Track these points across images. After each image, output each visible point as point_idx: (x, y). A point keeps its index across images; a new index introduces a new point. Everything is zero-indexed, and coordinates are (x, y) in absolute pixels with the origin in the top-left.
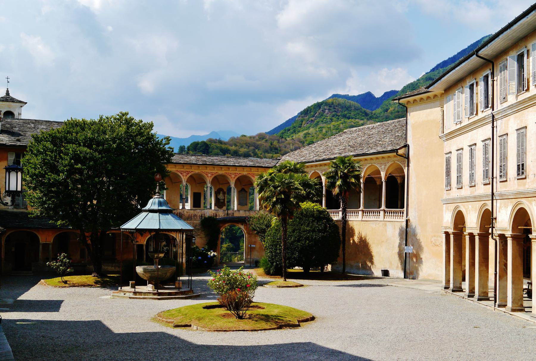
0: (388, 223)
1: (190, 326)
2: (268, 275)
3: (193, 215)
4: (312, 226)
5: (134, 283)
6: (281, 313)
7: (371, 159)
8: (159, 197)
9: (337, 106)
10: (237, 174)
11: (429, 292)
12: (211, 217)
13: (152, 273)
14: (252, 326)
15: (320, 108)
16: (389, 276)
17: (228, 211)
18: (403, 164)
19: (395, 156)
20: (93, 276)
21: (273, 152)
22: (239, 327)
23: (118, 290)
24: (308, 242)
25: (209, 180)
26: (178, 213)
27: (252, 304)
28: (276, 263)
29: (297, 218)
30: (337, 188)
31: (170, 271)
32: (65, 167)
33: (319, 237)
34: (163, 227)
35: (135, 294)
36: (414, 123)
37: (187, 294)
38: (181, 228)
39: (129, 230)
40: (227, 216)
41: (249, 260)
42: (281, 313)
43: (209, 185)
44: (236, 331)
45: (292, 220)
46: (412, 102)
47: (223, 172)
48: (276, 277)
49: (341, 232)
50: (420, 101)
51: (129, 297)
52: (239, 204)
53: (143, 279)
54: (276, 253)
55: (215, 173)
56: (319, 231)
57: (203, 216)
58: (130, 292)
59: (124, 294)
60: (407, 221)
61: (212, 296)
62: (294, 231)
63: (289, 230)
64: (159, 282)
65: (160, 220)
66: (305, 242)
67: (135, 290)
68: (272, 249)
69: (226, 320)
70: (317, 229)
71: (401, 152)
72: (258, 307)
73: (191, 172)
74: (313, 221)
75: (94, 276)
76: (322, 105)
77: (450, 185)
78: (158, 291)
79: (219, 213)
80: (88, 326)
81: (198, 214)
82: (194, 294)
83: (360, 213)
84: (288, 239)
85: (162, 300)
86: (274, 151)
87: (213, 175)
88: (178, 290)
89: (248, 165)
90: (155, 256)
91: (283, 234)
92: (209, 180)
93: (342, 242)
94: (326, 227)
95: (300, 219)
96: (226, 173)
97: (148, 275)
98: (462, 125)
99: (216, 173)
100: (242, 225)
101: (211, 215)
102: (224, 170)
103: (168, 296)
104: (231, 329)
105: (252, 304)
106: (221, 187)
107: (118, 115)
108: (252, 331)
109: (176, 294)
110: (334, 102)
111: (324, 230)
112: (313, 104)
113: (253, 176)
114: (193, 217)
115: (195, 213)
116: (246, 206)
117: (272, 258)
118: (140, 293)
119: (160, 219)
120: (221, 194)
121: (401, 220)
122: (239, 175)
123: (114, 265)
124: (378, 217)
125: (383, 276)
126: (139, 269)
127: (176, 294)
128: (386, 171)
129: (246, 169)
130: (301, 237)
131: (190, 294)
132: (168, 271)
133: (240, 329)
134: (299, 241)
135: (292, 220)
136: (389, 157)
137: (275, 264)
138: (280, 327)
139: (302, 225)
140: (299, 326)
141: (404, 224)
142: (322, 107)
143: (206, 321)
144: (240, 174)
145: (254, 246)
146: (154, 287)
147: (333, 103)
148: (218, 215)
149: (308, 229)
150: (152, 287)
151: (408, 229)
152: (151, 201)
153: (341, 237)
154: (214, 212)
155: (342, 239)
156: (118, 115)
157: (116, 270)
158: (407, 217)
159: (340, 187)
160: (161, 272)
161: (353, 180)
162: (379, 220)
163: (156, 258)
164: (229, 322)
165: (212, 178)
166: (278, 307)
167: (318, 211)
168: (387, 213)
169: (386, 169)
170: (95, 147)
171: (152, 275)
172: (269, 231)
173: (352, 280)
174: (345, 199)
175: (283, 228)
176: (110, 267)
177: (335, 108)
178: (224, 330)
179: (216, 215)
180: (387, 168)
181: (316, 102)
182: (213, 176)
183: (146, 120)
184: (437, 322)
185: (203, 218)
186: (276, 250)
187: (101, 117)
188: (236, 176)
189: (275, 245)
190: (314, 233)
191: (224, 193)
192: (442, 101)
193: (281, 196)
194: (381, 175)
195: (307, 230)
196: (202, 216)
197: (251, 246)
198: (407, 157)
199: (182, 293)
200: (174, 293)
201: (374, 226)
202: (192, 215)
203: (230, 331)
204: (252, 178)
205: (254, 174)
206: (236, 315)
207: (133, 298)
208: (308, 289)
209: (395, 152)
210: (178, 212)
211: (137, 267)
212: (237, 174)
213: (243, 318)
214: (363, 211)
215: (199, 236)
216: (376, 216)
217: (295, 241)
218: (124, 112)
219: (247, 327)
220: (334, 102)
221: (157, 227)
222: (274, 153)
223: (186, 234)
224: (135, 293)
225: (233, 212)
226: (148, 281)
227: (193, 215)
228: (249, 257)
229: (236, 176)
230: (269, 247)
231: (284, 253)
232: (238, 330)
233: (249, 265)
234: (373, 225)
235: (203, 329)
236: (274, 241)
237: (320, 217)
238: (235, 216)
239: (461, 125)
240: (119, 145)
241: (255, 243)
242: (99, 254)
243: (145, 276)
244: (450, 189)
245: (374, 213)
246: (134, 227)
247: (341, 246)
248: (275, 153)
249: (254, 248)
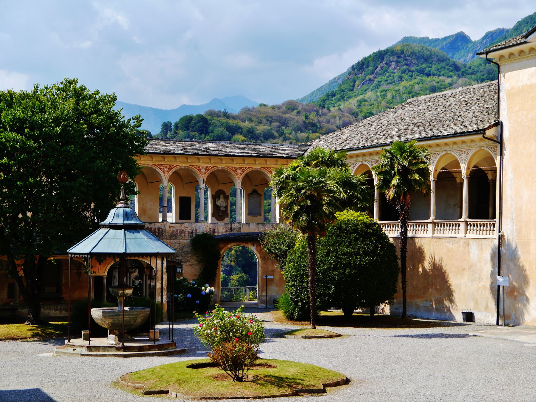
0: (471, 242)
1: (167, 392)
2: (291, 320)
3: (178, 232)
4: (355, 247)
5: (89, 333)
6: (299, 374)
7: (446, 144)
8: (124, 205)
9: (409, 56)
10: (244, 168)
11: (530, 346)
12: (206, 233)
13: (114, 317)
14: (254, 392)
15: (382, 59)
16: (474, 322)
17: (231, 225)
18: (494, 151)
19: (481, 139)
20: (27, 325)
21: (309, 130)
22: (237, 393)
24: (348, 270)
25: (202, 179)
26: (157, 229)
27: (258, 362)
28: (302, 301)
29: (333, 234)
30: (392, 189)
31: (141, 315)
33: (365, 262)
34: (130, 251)
35: (89, 350)
36: (509, 89)
37: (166, 349)
38: (157, 252)
39: (81, 256)
40: (231, 232)
41: (264, 298)
42: (299, 374)
43: (203, 185)
44: (232, 398)
45: (325, 238)
46: (507, 57)
47: (224, 166)
48: (303, 323)
49: (399, 254)
50: (519, 56)
51: (81, 354)
52: (250, 213)
53: (101, 327)
54: (302, 287)
55: (212, 168)
56: (366, 253)
57: (193, 232)
58: (83, 346)
59: (74, 350)
60: (501, 238)
61: (203, 352)
62: (327, 254)
63: (321, 251)
64: (125, 331)
65: (127, 240)
66: (345, 270)
67: (89, 344)
68: (296, 281)
69: (218, 383)
70: (363, 252)
71: (489, 133)
72: (267, 365)
73: (175, 167)
74: (357, 239)
75: (29, 324)
76: (386, 56)
78: (123, 345)
79: (218, 227)
80: (19, 394)
81: (187, 230)
82: (177, 347)
83: (430, 226)
84: (320, 267)
85: (129, 357)
86: (311, 130)
87: (208, 170)
88: (153, 343)
89: (262, 155)
90: (119, 293)
91: (310, 258)
92: (202, 179)
93: (400, 270)
94: (376, 247)
95: (338, 235)
96: (229, 167)
97: (109, 321)
99: (214, 167)
100: (253, 245)
101: (207, 231)
102: (225, 163)
103: (138, 351)
104: (224, 397)
105: (258, 362)
106: (221, 187)
107: (62, 83)
108: (255, 398)
109: (150, 348)
110: (406, 49)
111: (373, 253)
112: (371, 53)
113: (269, 172)
114: (178, 235)
115: (182, 228)
116: (259, 217)
117: (295, 295)
118: (98, 348)
119: (126, 238)
120: (222, 199)
121: (491, 236)
122: (249, 170)
123: (59, 307)
124: (457, 231)
125: (464, 321)
126: (96, 313)
127: (150, 348)
128: (467, 162)
129: (258, 161)
130: (339, 262)
131: (170, 348)
132: (138, 314)
133: (238, 396)
134: (335, 269)
135: (325, 238)
136: (472, 141)
137: (300, 303)
138: (296, 394)
139: (339, 245)
140: (324, 391)
141: (496, 242)
142: (385, 58)
143: (190, 385)
144: (249, 168)
145: (272, 277)
146: (117, 339)
147: (403, 52)
148: (216, 230)
149: (350, 250)
150: (115, 339)
151: (503, 250)
152: (112, 212)
153: (399, 262)
154: (211, 226)
155: (400, 266)
156: (62, 83)
157: (63, 316)
158: (499, 232)
159: (397, 186)
160: (128, 316)
161: (417, 177)
162: (458, 236)
163: (120, 296)
164: (223, 386)
165: (207, 175)
166: (296, 364)
167: (364, 223)
168: (471, 226)
169: (469, 159)
170: (28, 131)
171: (115, 320)
172: (292, 254)
173: (416, 327)
174: (404, 206)
175: (311, 250)
176: (54, 311)
177: (406, 60)
178: (215, 397)
179: (214, 231)
180: (470, 157)
181: (376, 50)
182: (209, 172)
183: (105, 91)
184: (530, 387)
185: (194, 236)
186: (302, 282)
187: (36, 87)
188: (244, 171)
189: (300, 274)
190: (358, 257)
191: (226, 198)
193: (306, 202)
194: (460, 168)
195: (347, 252)
196: (192, 233)
197: (266, 277)
199: (160, 347)
200: (148, 347)
201: (451, 246)
202: (177, 231)
203: (223, 398)
204: (268, 174)
205: (270, 168)
206: (233, 376)
207: (87, 355)
208: (347, 340)
209: (481, 133)
210: (157, 228)
211: (92, 310)
212: (244, 168)
213: (243, 380)
214: (434, 223)
215: (188, 263)
216: (454, 230)
217: (329, 269)
218: (71, 78)
219: (247, 393)
220: (406, 49)
221: (121, 250)
222: (311, 131)
223: (167, 260)
224: (90, 348)
225: (239, 227)
226: (109, 330)
228: (264, 294)
229: (243, 171)
230: (291, 278)
231: (313, 287)
232: (234, 397)
233: (264, 305)
234: (450, 245)
235: (185, 397)
236: (298, 270)
237: (366, 233)
238: (242, 232)
240: (64, 130)
241: (273, 272)
242: (36, 292)
243: (104, 322)
245: (451, 226)
246: (87, 250)
247: (400, 276)
248: (313, 132)
249: (272, 280)
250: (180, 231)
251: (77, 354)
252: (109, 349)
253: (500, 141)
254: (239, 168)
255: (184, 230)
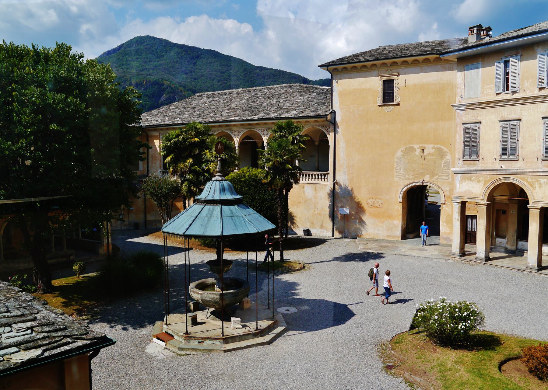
0: (306, 186)
18: (326, 129)
32: (26, 127)
50: (351, 70)
66: (267, 212)
77: (479, 156)
98: (516, 96)
158: (334, 180)
192: (381, 71)
198: (333, 121)
209: (324, 117)
239: (514, 95)
244: (478, 159)
251: (219, 351)
252: (246, 337)
253: (334, 124)
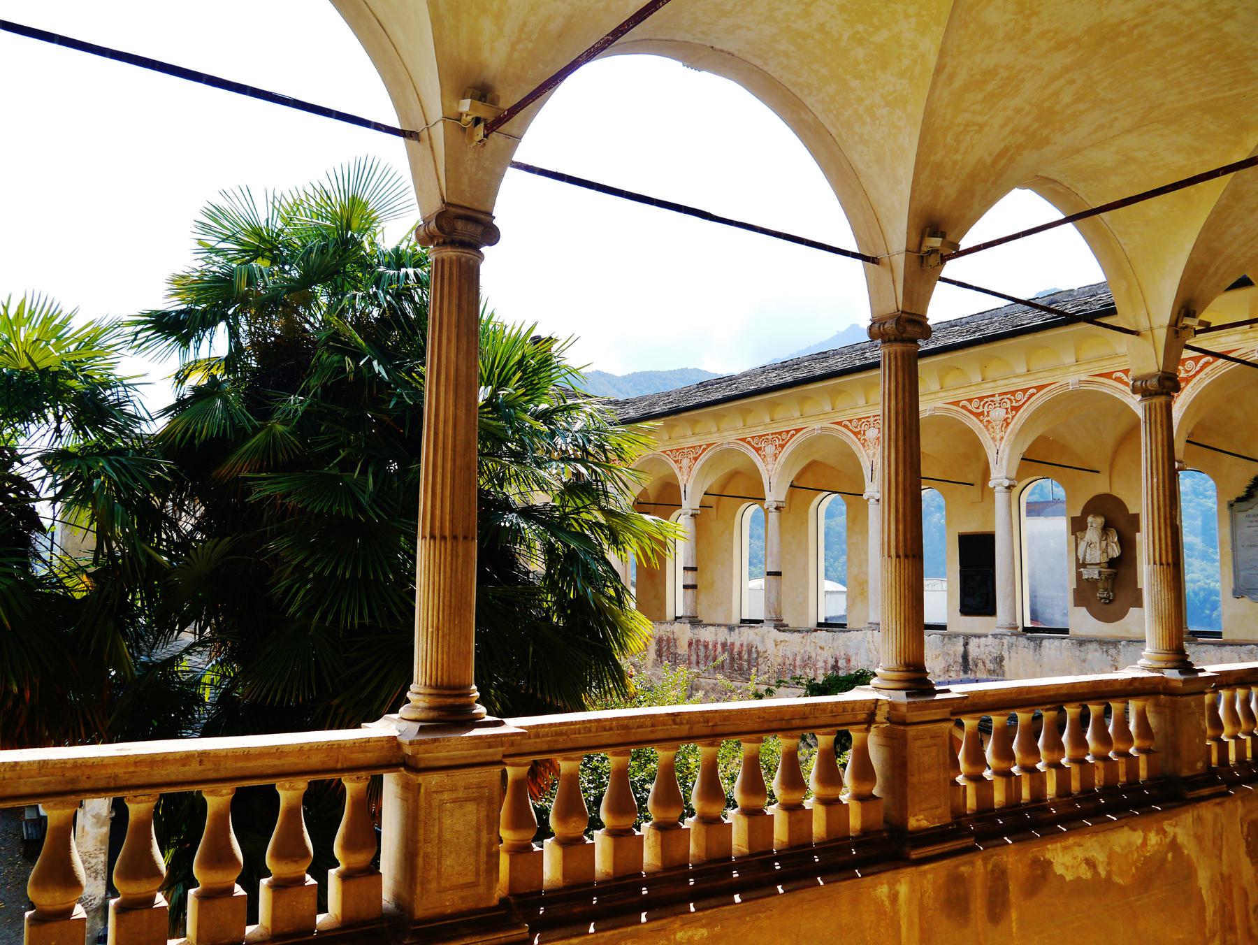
10: (1019, 396)
23: (639, 922)
40: (965, 672)
57: (839, 665)
96: (956, 403)
115: (808, 648)
144: (1039, 388)
212: (1019, 396)
227: (798, 658)
229: (1013, 408)
250: (803, 660)
254: (997, 398)
255: (813, 655)
